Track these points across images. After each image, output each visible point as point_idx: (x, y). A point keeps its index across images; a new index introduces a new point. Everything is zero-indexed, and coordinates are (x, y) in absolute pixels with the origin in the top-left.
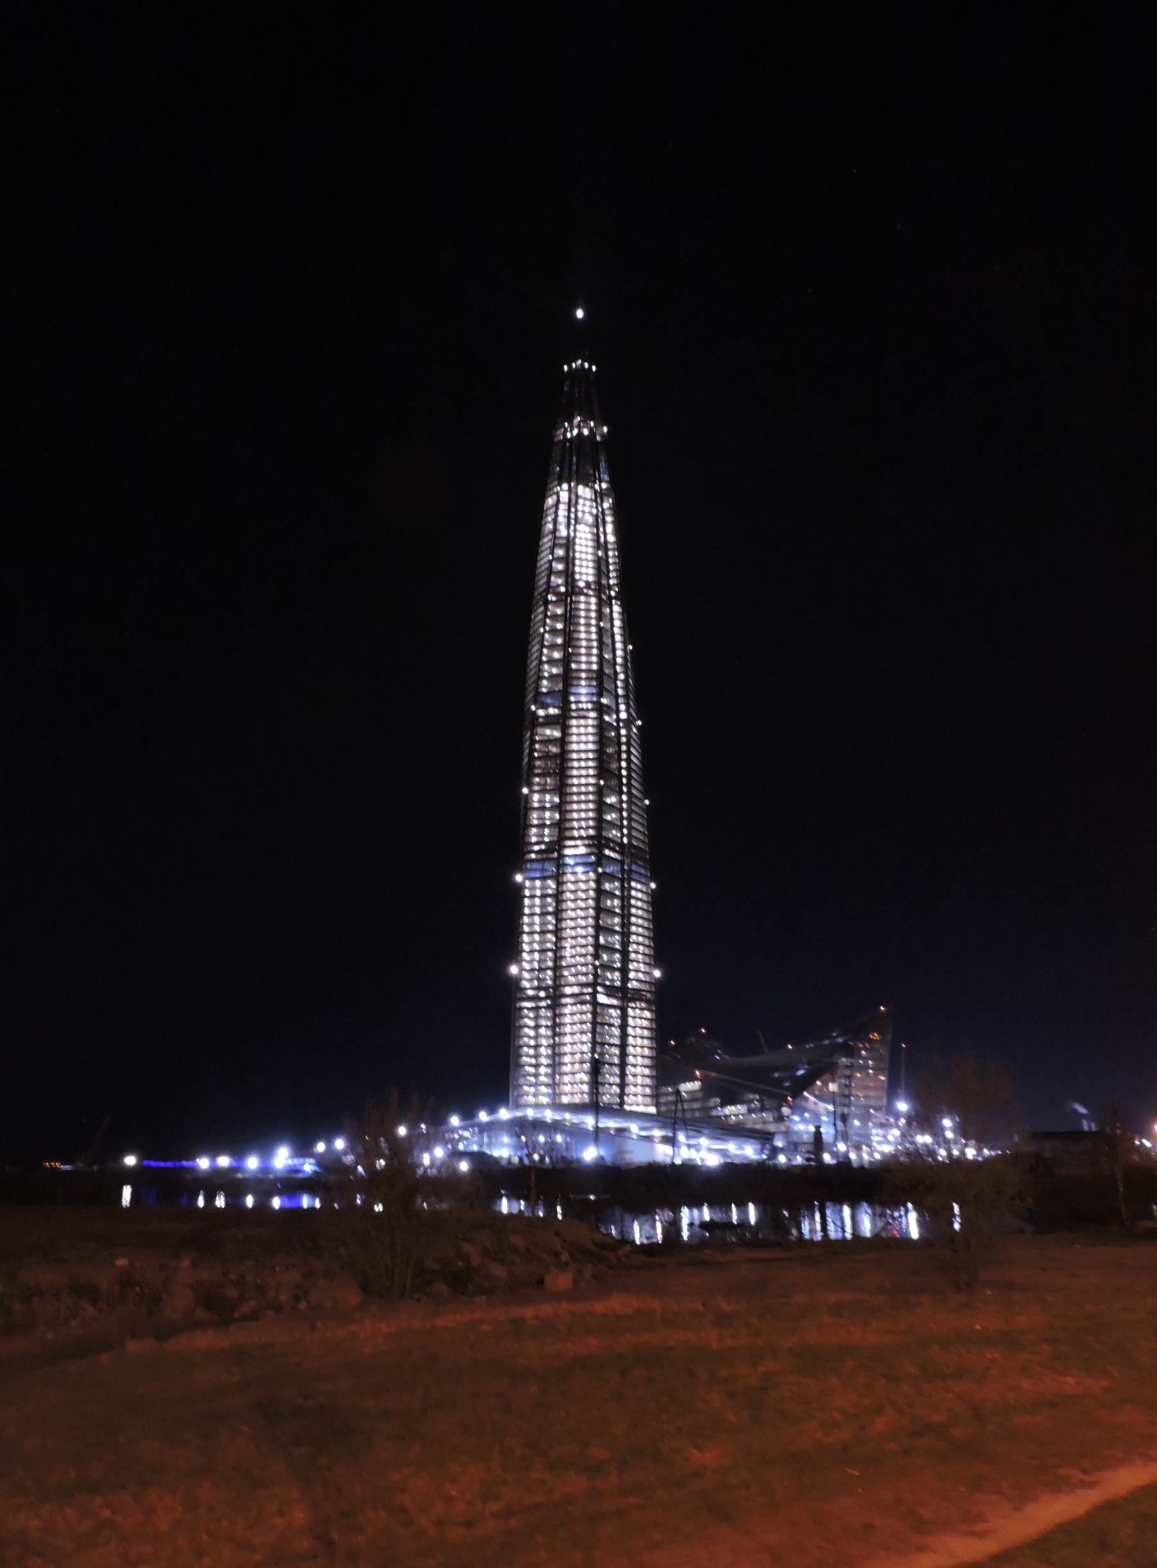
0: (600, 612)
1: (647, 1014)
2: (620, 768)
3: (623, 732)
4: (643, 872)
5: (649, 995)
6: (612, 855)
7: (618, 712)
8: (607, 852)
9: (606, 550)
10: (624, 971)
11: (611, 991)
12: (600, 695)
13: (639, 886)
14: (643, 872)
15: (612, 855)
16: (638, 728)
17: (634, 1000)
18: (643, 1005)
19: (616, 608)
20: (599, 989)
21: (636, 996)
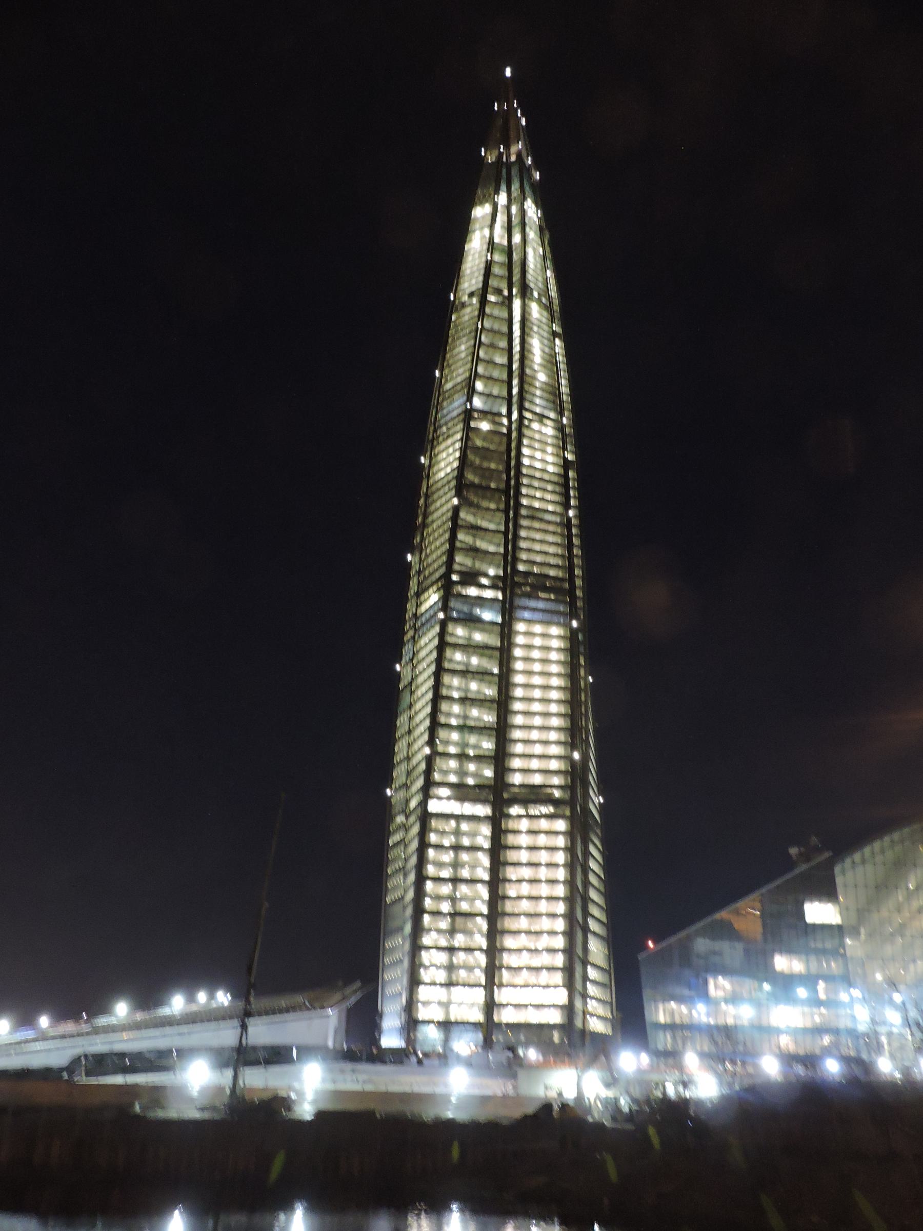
0: (482, 313)
1: (561, 825)
2: (509, 478)
3: (514, 435)
4: (562, 608)
5: (557, 794)
6: (489, 594)
7: (509, 415)
8: (472, 591)
9: (509, 251)
10: (500, 758)
11: (462, 792)
12: (470, 399)
13: (555, 630)
14: (562, 608)
15: (489, 594)
16: (560, 428)
17: (525, 802)
18: (551, 809)
19: (517, 304)
20: (444, 792)
21: (533, 795)
